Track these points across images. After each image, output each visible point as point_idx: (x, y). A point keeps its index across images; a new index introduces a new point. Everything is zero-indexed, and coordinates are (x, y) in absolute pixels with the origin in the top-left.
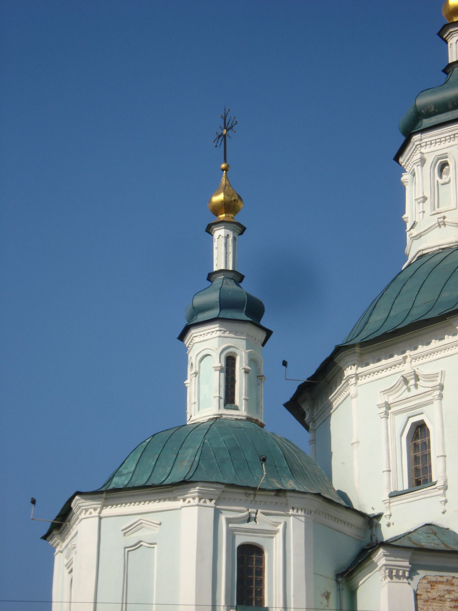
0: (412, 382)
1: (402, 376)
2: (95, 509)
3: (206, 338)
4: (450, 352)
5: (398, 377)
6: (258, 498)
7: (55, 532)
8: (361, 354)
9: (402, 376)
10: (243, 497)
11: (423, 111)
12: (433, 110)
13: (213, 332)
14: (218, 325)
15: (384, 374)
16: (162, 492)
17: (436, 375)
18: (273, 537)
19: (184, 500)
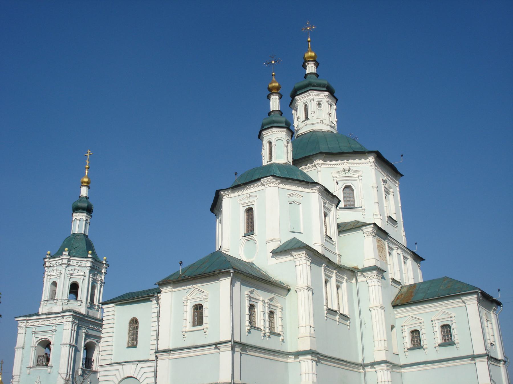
0: (347, 172)
1: (344, 169)
2: (276, 184)
3: (279, 133)
4: (364, 165)
5: (342, 169)
6: (328, 197)
7: (231, 189)
8: (324, 157)
9: (344, 169)
10: (325, 195)
11: (312, 84)
12: (316, 85)
13: (283, 132)
14: (286, 130)
15: (334, 166)
16: (304, 185)
17: (359, 171)
18: (330, 212)
19: (312, 190)
